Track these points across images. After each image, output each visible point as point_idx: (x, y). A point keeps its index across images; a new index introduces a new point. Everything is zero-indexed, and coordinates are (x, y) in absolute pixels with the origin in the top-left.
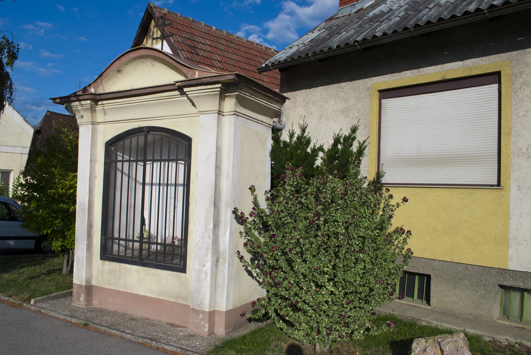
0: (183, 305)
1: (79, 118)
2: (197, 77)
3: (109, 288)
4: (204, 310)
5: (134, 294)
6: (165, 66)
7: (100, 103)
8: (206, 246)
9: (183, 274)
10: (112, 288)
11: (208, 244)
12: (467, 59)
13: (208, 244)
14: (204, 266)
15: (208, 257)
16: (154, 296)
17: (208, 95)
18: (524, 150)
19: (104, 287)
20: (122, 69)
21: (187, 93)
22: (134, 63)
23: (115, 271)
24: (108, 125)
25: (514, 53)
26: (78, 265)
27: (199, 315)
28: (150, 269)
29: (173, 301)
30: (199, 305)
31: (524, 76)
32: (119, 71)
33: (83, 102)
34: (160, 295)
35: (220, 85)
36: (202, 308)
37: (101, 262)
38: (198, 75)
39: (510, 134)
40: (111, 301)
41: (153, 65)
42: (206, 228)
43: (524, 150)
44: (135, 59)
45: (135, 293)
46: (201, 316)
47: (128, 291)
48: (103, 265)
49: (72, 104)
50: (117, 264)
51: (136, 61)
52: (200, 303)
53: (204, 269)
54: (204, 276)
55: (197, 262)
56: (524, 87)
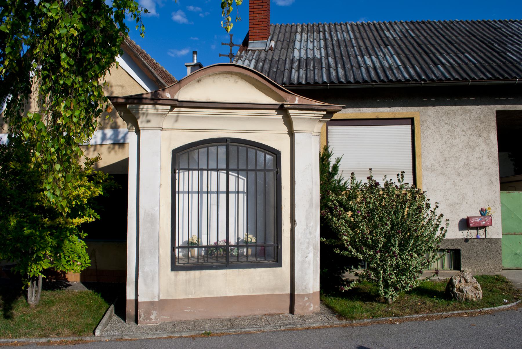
1: (142, 122)
2: (296, 102)
5: (221, 297)
6: (251, 85)
7: (176, 109)
8: (307, 240)
9: (280, 268)
10: (190, 297)
11: (309, 239)
12: (393, 107)
13: (309, 239)
14: (306, 257)
15: (310, 249)
18: (429, 167)
19: (177, 298)
20: (202, 79)
22: (217, 77)
23: (195, 279)
24: (174, 133)
25: (422, 108)
26: (145, 281)
27: (304, 299)
28: (241, 270)
29: (269, 293)
30: (303, 290)
31: (428, 123)
32: (199, 81)
33: (158, 107)
34: (254, 291)
35: (325, 113)
37: (173, 273)
38: (299, 101)
39: (421, 157)
42: (307, 226)
43: (429, 167)
46: (306, 299)
48: (176, 276)
49: (141, 107)
50: (197, 273)
52: (304, 288)
53: (307, 259)
55: (300, 255)
56: (428, 129)
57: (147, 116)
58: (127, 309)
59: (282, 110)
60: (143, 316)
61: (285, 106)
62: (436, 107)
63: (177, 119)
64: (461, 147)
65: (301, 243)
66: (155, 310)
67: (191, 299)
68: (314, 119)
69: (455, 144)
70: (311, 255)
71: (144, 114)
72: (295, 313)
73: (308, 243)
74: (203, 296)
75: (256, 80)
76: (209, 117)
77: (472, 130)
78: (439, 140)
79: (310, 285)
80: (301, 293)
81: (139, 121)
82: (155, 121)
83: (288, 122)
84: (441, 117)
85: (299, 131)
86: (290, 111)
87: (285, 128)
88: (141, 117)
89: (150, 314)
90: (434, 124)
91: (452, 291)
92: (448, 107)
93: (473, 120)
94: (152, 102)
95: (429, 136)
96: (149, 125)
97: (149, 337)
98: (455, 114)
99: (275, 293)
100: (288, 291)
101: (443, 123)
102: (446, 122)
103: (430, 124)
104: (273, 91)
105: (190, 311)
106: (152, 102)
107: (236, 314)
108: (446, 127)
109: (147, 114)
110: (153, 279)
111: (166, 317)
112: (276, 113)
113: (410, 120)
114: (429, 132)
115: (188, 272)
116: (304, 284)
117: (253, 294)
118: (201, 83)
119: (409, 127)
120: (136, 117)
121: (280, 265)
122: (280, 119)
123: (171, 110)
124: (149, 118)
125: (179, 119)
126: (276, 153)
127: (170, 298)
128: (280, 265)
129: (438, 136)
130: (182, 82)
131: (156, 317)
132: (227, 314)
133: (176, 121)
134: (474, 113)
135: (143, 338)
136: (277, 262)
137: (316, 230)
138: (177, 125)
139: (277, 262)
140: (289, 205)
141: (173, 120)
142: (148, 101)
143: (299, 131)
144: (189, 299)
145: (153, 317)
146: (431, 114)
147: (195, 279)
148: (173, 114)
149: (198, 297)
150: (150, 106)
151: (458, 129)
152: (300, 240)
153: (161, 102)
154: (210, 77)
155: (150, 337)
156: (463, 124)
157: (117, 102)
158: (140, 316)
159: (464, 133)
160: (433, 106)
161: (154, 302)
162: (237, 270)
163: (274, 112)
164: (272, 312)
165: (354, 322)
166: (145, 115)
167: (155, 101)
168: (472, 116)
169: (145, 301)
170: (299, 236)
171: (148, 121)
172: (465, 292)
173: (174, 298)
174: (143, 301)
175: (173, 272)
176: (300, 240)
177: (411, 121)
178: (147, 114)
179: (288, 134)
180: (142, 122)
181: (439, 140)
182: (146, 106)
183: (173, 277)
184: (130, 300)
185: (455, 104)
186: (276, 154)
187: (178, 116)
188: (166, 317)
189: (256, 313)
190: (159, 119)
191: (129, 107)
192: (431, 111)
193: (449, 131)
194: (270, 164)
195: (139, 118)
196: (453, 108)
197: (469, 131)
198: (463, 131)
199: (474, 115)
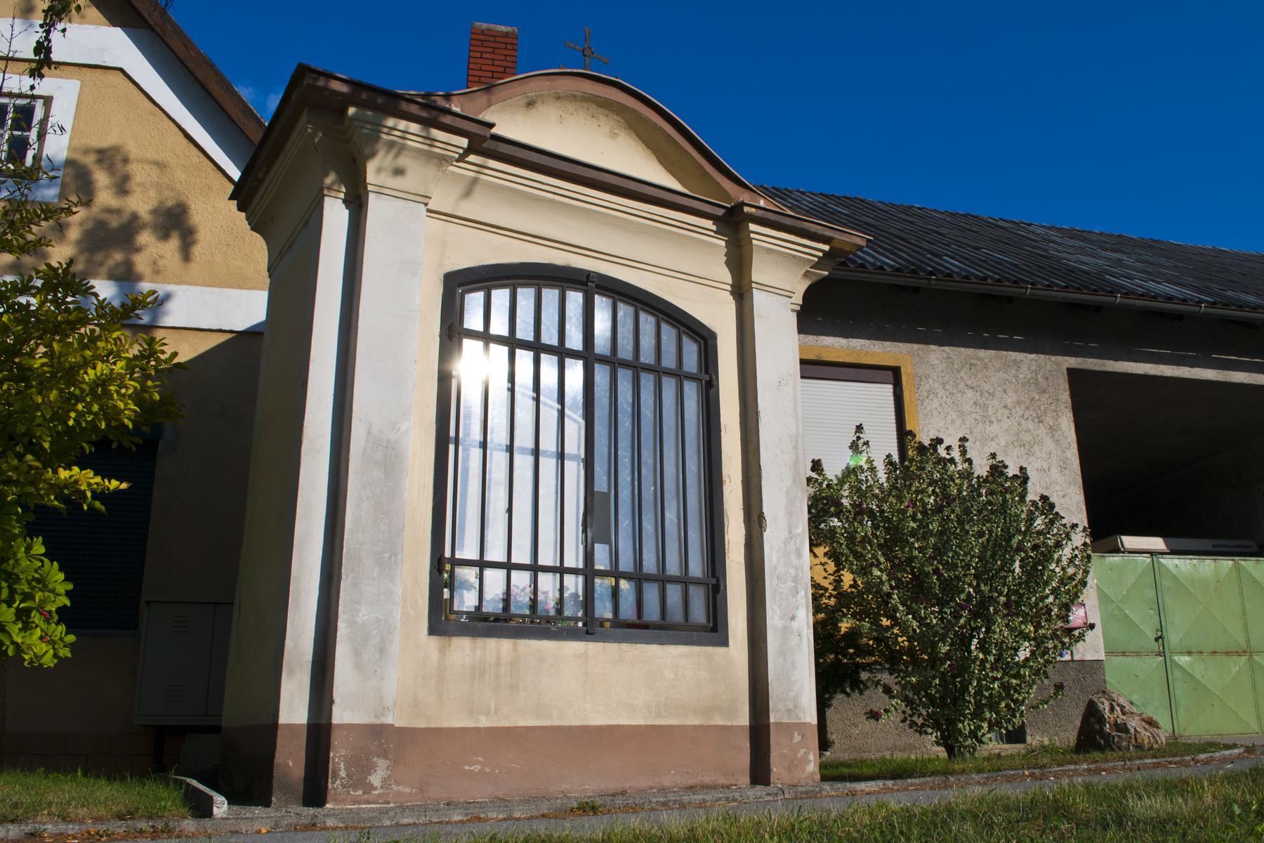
0: (724, 728)
1: (379, 170)
3: (473, 725)
5: (571, 728)
8: (793, 572)
9: (723, 649)
10: (484, 722)
11: (797, 568)
12: (852, 337)
14: (793, 618)
16: (641, 722)
17: (794, 256)
19: (445, 725)
20: (539, 102)
21: (752, 236)
23: (498, 665)
24: (454, 229)
25: (916, 346)
26: (357, 653)
29: (697, 722)
30: (789, 711)
32: (530, 104)
33: (435, 133)
34: (659, 715)
35: (826, 248)
36: (798, 717)
37: (435, 641)
40: (477, 768)
41: (614, 136)
42: (790, 532)
44: (573, 98)
45: (576, 722)
48: (442, 651)
49: (391, 122)
51: (585, 105)
52: (791, 706)
53: (795, 624)
54: (794, 642)
56: (932, 396)
57: (397, 155)
58: (278, 759)
59: (732, 223)
60: (343, 774)
61: (746, 209)
62: (947, 349)
63: (470, 189)
64: (1003, 443)
65: (779, 578)
66: (385, 755)
67: (486, 729)
69: (992, 435)
71: (391, 145)
72: (773, 778)
74: (521, 723)
75: (669, 136)
76: (553, 201)
77: (1023, 407)
78: (958, 423)
80: (785, 720)
81: (371, 167)
82: (418, 175)
83: (739, 262)
84: (958, 371)
85: (765, 287)
86: (752, 227)
87: (726, 276)
88: (381, 154)
89: (371, 768)
90: (944, 385)
91: (1101, 732)
92: (971, 350)
93: (1023, 385)
94: (425, 114)
95: (935, 413)
96: (398, 182)
97: (406, 821)
98: (986, 367)
99: (713, 723)
100: (744, 719)
101: (962, 386)
102: (969, 383)
103: (936, 385)
104: (705, 173)
105: (482, 771)
106: (425, 114)
107: (612, 786)
108: (970, 394)
109: (403, 148)
110: (382, 650)
111: (408, 790)
112: (714, 228)
113: (891, 373)
114: (935, 404)
115: (481, 641)
116: (792, 694)
117: (657, 722)
118: (534, 112)
119: (889, 388)
120: (367, 151)
121: (724, 642)
122: (719, 246)
123: (469, 150)
124: (404, 161)
125: (478, 190)
126: (705, 335)
127: (421, 724)
128: (724, 642)
129: (953, 415)
130: (495, 90)
131: (384, 781)
132: (584, 782)
133: (467, 194)
134: (1024, 368)
135: (388, 823)
136: (713, 630)
138: (469, 209)
139: (713, 630)
140: (740, 477)
141: (459, 189)
142: (414, 109)
143: (765, 287)
144: (478, 730)
145: (375, 779)
146: (936, 362)
147: (498, 665)
148: (464, 171)
149: (506, 724)
150: (414, 127)
151: (995, 403)
153: (448, 120)
154: (558, 104)
155: (411, 821)
156: (1005, 391)
157: (325, 88)
158: (336, 775)
159: (1007, 412)
160: (941, 345)
163: (709, 224)
164: (707, 780)
165: (951, 779)
166: (395, 151)
167: (435, 113)
168: (1021, 376)
169: (355, 722)
170: (774, 558)
171: (399, 172)
172: (1132, 730)
173: (432, 725)
174: (346, 721)
175: (433, 638)
176: (776, 568)
177: (894, 375)
178: (403, 148)
179: (732, 293)
180: (379, 170)
181: (958, 423)
182: (402, 124)
183: (435, 656)
184: (291, 727)
185: (985, 346)
186: (705, 339)
187: (475, 181)
188: (408, 790)
189: (667, 782)
190: (430, 171)
191: (356, 114)
192: (936, 355)
193: (975, 403)
194: (691, 362)
195: (373, 155)
196: (982, 353)
197: (1018, 409)
198: (1005, 407)
199: (1024, 373)
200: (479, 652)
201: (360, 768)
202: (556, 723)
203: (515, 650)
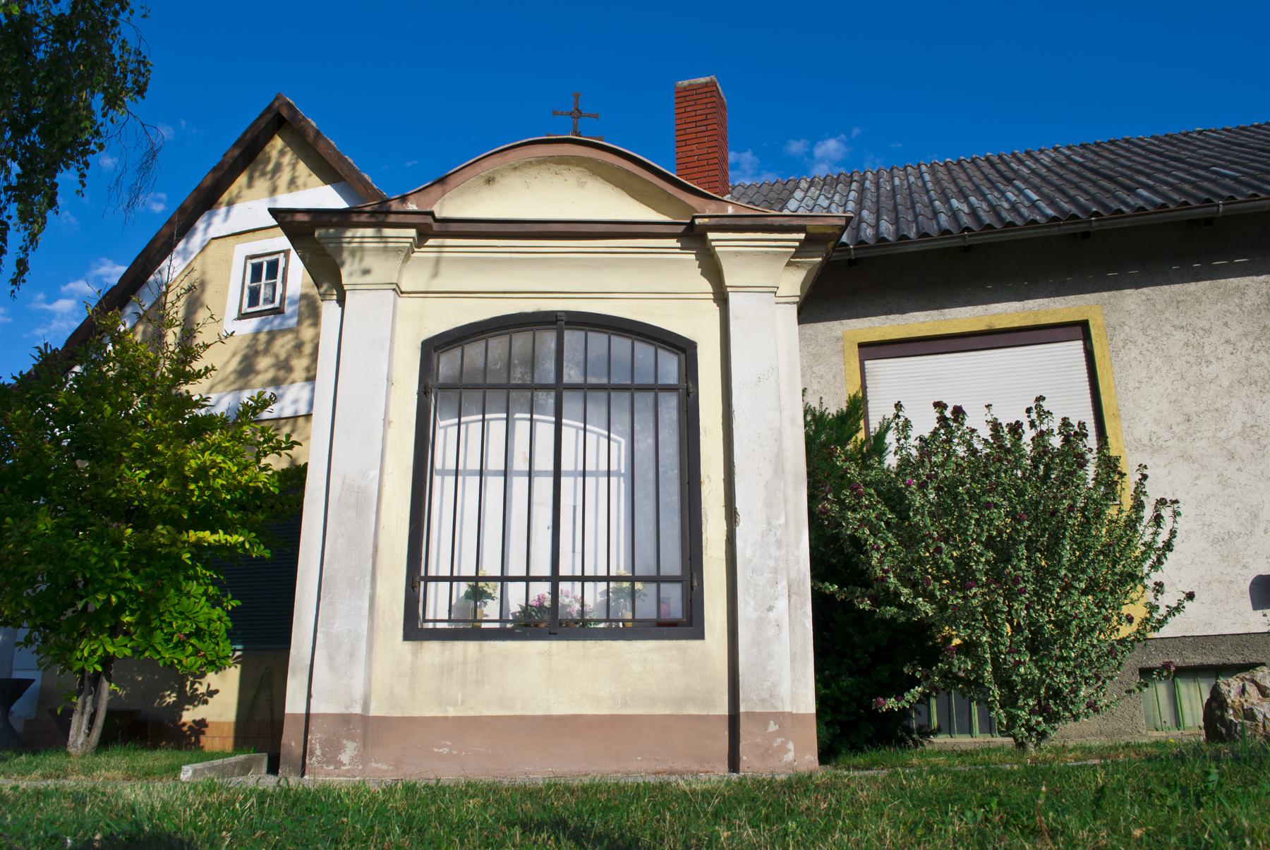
0: (700, 717)
3: (442, 714)
4: (781, 710)
5: (533, 718)
6: (619, 190)
7: (431, 242)
8: (772, 563)
10: (451, 712)
11: (776, 559)
12: (1028, 298)
13: (776, 559)
14: (770, 609)
15: (780, 586)
17: (766, 253)
18: (1145, 441)
19: (417, 714)
20: (498, 178)
21: (714, 244)
22: (533, 171)
23: (465, 663)
24: (431, 302)
25: (1106, 294)
26: (331, 658)
27: (766, 726)
28: (589, 643)
29: (667, 712)
30: (763, 701)
31: (1127, 329)
32: (490, 181)
33: (388, 232)
34: (625, 704)
35: (802, 236)
36: (774, 707)
37: (409, 645)
39: (1119, 416)
40: (446, 750)
41: (582, 185)
42: (769, 524)
43: (1145, 441)
46: (773, 727)
47: (511, 713)
48: (415, 653)
49: (349, 233)
51: (544, 166)
52: (765, 695)
53: (772, 615)
55: (752, 603)
56: (1129, 345)
57: (361, 260)
58: (285, 740)
59: (693, 236)
60: (318, 752)
62: (1145, 290)
64: (1226, 383)
68: (775, 253)
69: (1210, 377)
70: (782, 604)
73: (775, 570)
74: (486, 713)
75: (628, 172)
76: (511, 259)
77: (1251, 338)
78: (1164, 370)
79: (785, 688)
80: (758, 710)
81: (344, 272)
82: (383, 269)
83: (712, 269)
84: (1162, 312)
86: (711, 235)
87: (707, 286)
89: (339, 749)
90: (1144, 331)
91: (1222, 720)
92: (1177, 286)
93: (1251, 313)
95: (1134, 363)
96: (368, 279)
98: (1199, 301)
99: (685, 713)
100: (723, 709)
101: (1168, 328)
102: (1177, 322)
103: (1134, 332)
104: (670, 196)
108: (1178, 335)
110: (352, 655)
111: (385, 767)
112: (679, 245)
113: (1079, 329)
114: (1134, 352)
115: (449, 644)
116: (767, 684)
117: (623, 712)
118: (497, 186)
119: (1078, 345)
120: (338, 261)
121: (700, 635)
124: (369, 262)
125: (443, 267)
128: (700, 635)
129: (1158, 362)
131: (352, 759)
134: (1251, 293)
136: (688, 624)
137: (798, 542)
138: (437, 285)
139: (688, 624)
141: (428, 271)
142: (364, 218)
144: (446, 718)
145: (345, 758)
146: (1133, 307)
147: (465, 663)
148: (425, 254)
149: (472, 713)
150: (369, 232)
151: (1213, 339)
152: (750, 561)
153: (392, 218)
154: (518, 173)
156: (1226, 324)
157: (292, 222)
158: (312, 753)
159: (1230, 348)
160: (1137, 287)
161: (351, 715)
162: (580, 643)
163: (673, 242)
166: (358, 255)
168: (1246, 304)
169: (329, 711)
170: (749, 552)
171: (366, 272)
172: (1260, 717)
176: (750, 561)
177: (1081, 330)
179: (715, 300)
180: (351, 274)
181: (1164, 370)
182: (360, 232)
183: (408, 658)
184: (294, 716)
185: (1197, 278)
186: (685, 349)
188: (385, 767)
189: (633, 767)
192: (1132, 300)
193: (1187, 345)
195: (343, 264)
196: (1192, 286)
197: (1245, 342)
198: (1227, 342)
199: (1252, 299)
200: (447, 654)
201: (333, 748)
202: (519, 713)
203: (480, 651)
